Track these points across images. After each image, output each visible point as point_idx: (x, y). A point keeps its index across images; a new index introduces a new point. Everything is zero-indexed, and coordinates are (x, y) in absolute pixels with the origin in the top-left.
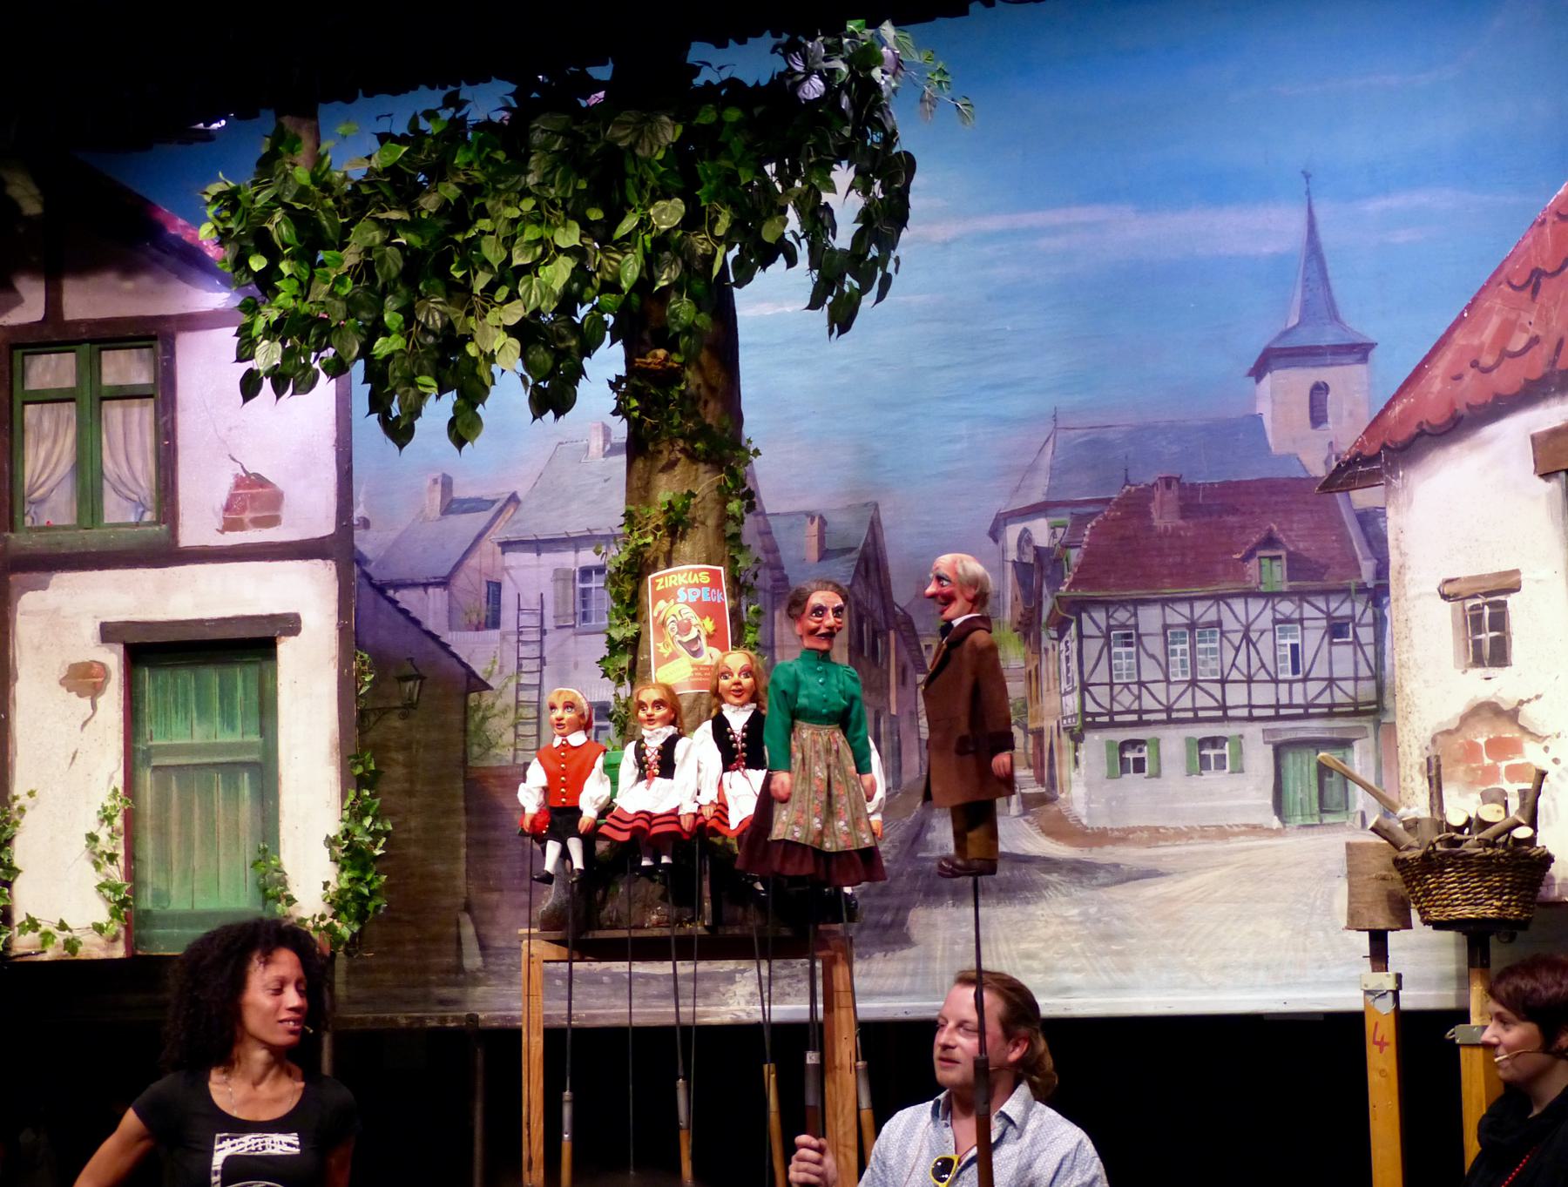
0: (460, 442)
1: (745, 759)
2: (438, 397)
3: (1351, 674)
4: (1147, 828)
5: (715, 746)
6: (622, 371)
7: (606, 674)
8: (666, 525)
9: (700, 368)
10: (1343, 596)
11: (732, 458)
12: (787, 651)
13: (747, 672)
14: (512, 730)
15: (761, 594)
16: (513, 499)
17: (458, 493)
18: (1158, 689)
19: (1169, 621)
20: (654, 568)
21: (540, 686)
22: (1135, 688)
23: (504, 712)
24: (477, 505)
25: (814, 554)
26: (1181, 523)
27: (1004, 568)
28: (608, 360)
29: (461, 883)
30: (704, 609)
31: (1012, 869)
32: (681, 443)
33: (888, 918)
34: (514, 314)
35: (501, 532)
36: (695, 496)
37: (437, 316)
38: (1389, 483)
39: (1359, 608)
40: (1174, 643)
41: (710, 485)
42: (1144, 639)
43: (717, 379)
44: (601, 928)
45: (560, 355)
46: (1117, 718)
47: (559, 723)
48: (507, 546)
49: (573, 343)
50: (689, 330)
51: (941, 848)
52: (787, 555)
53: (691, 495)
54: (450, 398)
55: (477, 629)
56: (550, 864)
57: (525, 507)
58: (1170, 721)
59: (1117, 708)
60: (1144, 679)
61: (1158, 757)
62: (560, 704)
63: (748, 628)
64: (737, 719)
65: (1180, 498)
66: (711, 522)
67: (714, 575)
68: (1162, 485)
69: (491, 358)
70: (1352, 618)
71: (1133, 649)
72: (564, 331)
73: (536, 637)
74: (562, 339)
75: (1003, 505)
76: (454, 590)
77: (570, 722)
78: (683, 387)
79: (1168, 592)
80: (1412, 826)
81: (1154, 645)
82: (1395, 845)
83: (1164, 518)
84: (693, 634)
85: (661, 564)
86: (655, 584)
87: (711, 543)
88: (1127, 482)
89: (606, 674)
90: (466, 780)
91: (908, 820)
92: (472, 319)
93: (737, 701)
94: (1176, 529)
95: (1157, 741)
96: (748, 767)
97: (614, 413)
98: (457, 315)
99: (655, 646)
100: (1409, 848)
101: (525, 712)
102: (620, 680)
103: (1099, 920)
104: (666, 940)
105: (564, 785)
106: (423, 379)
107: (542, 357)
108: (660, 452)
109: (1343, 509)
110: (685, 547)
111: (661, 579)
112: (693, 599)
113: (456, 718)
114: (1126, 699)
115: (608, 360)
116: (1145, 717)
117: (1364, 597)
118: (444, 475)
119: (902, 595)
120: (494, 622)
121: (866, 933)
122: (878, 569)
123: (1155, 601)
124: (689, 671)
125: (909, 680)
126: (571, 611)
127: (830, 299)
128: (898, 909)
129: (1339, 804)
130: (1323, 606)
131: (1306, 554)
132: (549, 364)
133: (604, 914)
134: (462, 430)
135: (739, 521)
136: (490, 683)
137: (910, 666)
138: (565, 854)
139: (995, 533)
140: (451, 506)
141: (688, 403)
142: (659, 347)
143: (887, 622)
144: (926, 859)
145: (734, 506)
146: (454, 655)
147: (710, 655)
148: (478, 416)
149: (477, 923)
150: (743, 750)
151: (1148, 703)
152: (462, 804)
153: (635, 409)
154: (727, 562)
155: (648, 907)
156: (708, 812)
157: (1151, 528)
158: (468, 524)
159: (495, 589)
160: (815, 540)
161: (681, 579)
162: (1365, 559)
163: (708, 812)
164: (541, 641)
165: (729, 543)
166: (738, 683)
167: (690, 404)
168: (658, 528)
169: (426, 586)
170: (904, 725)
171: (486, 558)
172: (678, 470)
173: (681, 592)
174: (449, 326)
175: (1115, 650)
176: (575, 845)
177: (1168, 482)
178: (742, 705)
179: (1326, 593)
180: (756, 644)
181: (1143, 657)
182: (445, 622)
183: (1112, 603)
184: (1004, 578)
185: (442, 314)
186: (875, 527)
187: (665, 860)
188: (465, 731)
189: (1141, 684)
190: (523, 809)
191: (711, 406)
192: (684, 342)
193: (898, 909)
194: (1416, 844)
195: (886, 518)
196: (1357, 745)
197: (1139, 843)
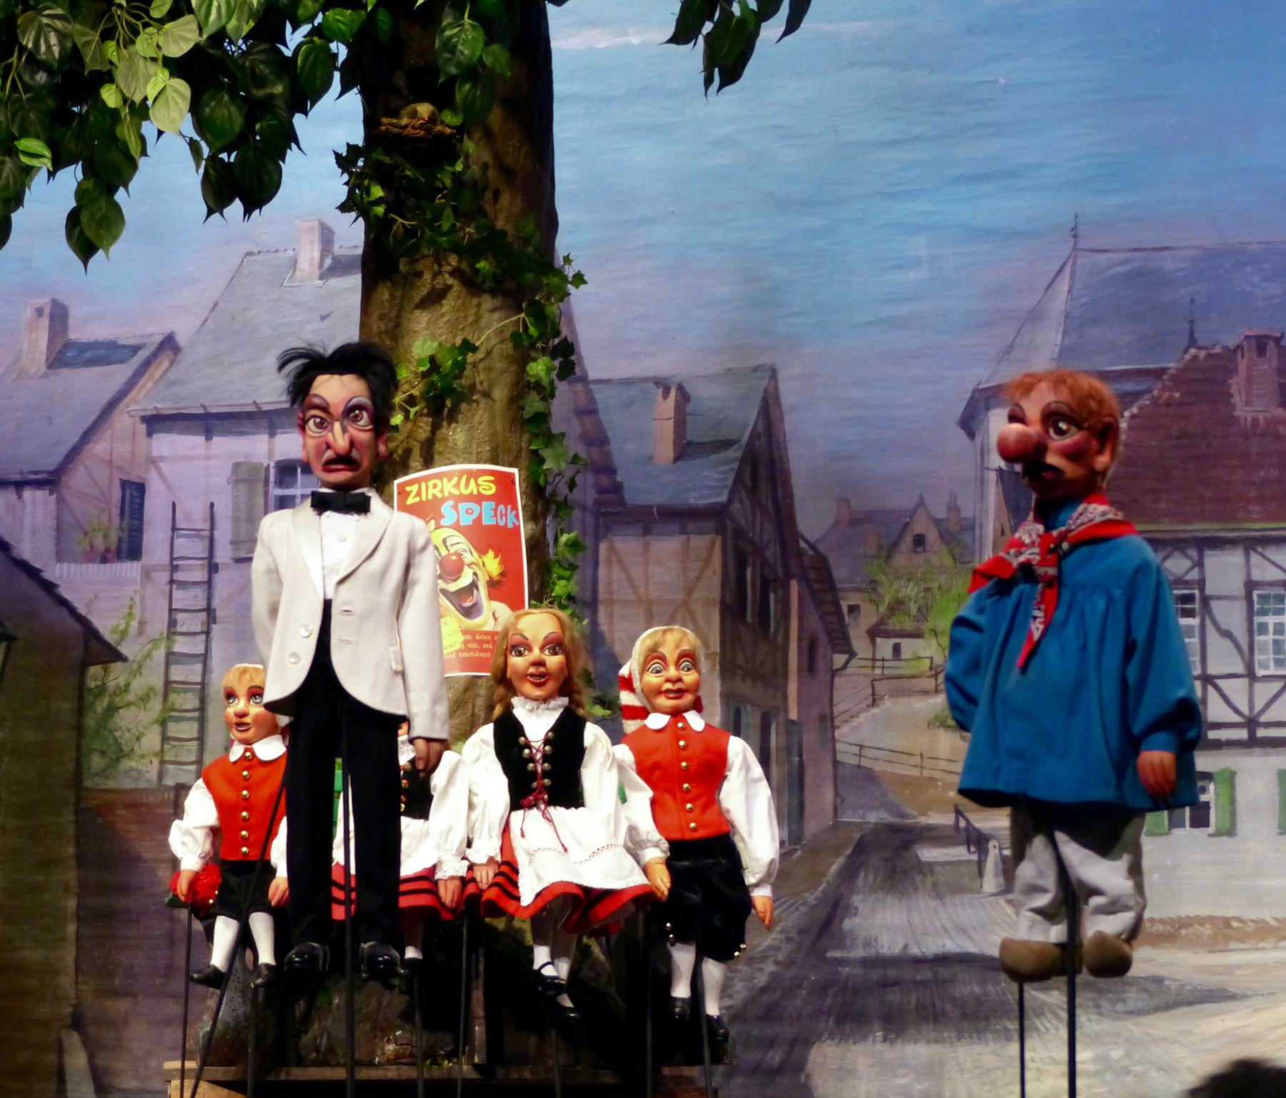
0: (85, 248)
1: (548, 789)
2: (51, 174)
4: (1211, 920)
5: (497, 767)
6: (358, 138)
8: (424, 396)
9: (488, 135)
11: (538, 287)
12: (617, 609)
13: (554, 644)
14: (156, 729)
15: (577, 513)
16: (169, 344)
17: (78, 332)
18: (1237, 689)
19: (1256, 576)
20: (404, 468)
21: (205, 658)
23: (145, 699)
24: (104, 353)
25: (666, 451)
27: (982, 480)
28: (335, 120)
29: (66, 982)
30: (484, 538)
31: (983, 982)
32: (453, 260)
33: (775, 1057)
34: (181, 39)
35: (145, 399)
36: (474, 349)
37: (53, 39)
40: (1264, 613)
41: (501, 331)
42: (1214, 605)
43: (515, 151)
44: (301, 1063)
45: (256, 109)
47: (240, 722)
48: (155, 422)
49: (279, 89)
50: (473, 72)
51: (867, 944)
52: (623, 450)
53: (468, 347)
54: (72, 176)
55: (104, 560)
56: (219, 957)
57: (186, 359)
58: (1253, 742)
60: (1211, 670)
61: (1232, 802)
62: (242, 690)
63: (557, 571)
64: (537, 724)
66: (500, 394)
67: (504, 482)
68: (1251, 353)
69: (141, 111)
71: (1195, 622)
72: (263, 69)
73: (201, 575)
74: (261, 82)
75: (981, 375)
76: (66, 493)
77: (257, 717)
78: (459, 167)
79: (1256, 527)
81: (1231, 615)
83: (1252, 403)
84: (466, 579)
85: (415, 461)
87: (499, 427)
88: (1192, 342)
90: (78, 811)
91: (811, 898)
92: (111, 48)
93: (538, 692)
95: (1230, 777)
96: (553, 802)
97: (344, 208)
98: (87, 37)
101: (178, 700)
103: (1127, 1071)
104: (409, 1085)
105: (246, 824)
106: (26, 144)
107: (227, 112)
108: (419, 275)
110: (456, 434)
112: (467, 521)
113: (65, 707)
115: (335, 120)
118: (55, 303)
119: (813, 520)
120: (131, 548)
121: (739, 1080)
122: (773, 479)
123: (1233, 542)
124: (461, 638)
125: (820, 664)
127: (708, 27)
128: (793, 1043)
132: (238, 123)
133: (306, 1039)
134: (90, 229)
135: (547, 393)
136: (124, 650)
137: (823, 638)
138: (245, 940)
139: (970, 422)
140: (65, 354)
141: (467, 195)
142: (421, 100)
143: (786, 566)
144: (842, 962)
145: (539, 368)
146: (64, 603)
147: (494, 615)
148: (117, 208)
149: (92, 1049)
150: (546, 774)
152: (71, 850)
153: (379, 201)
154: (525, 463)
155: (381, 1030)
156: (485, 877)
158: (93, 385)
159: (134, 495)
160: (669, 428)
161: (448, 487)
163: (485, 877)
164: (209, 583)
165: (527, 431)
166: (540, 663)
167: (472, 200)
168: (411, 401)
169: (19, 485)
170: (810, 738)
171: (121, 441)
172: (448, 304)
173: (447, 509)
174: (74, 55)
176: (261, 925)
177: (1261, 344)
178: (545, 700)
180: (570, 598)
181: (1212, 635)
182: (49, 546)
184: (983, 497)
185: (62, 36)
186: (770, 406)
187: (411, 953)
188: (79, 729)
190: (175, 862)
191: (505, 199)
192: (463, 91)
193: (793, 1043)
195: (789, 393)
197: (1196, 943)
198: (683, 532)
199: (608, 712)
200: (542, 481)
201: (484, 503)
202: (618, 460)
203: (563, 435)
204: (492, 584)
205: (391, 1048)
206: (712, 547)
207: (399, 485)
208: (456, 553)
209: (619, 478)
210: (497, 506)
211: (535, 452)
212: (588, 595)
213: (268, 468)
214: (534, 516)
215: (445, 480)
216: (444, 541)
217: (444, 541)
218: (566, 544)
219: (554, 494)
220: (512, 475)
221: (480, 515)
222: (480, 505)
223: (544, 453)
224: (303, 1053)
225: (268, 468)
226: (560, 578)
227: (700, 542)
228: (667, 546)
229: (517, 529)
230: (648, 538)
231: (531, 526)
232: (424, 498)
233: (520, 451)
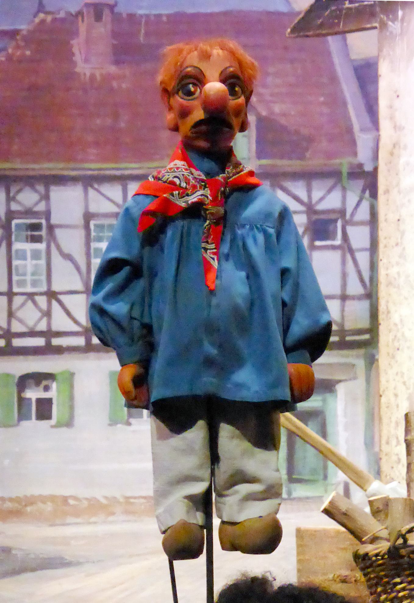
3: (338, 291)
4: (52, 498)
10: (330, 182)
19: (93, 209)
22: (42, 301)
26: (113, 69)
38: (383, 26)
39: (352, 199)
42: (58, 232)
46: (17, 342)
59: (17, 327)
60: (56, 287)
61: (71, 398)
65: (115, 34)
68: (89, 18)
70: (342, 212)
71: (41, 246)
79: (93, 167)
80: (381, 508)
81: (71, 241)
82: (356, 534)
83: (90, 59)
88: (41, 8)
94: (108, 78)
100: (374, 540)
109: (337, 60)
114: (29, 316)
116: (56, 342)
117: (360, 183)
123: (74, 180)
129: (314, 471)
130: (302, 194)
131: (283, 121)
151: (60, 321)
157: (71, 76)
162: (362, 130)
175: (17, 246)
179: (308, 176)
183: (17, 179)
189: (51, 295)
194: (384, 534)
196: (341, 389)
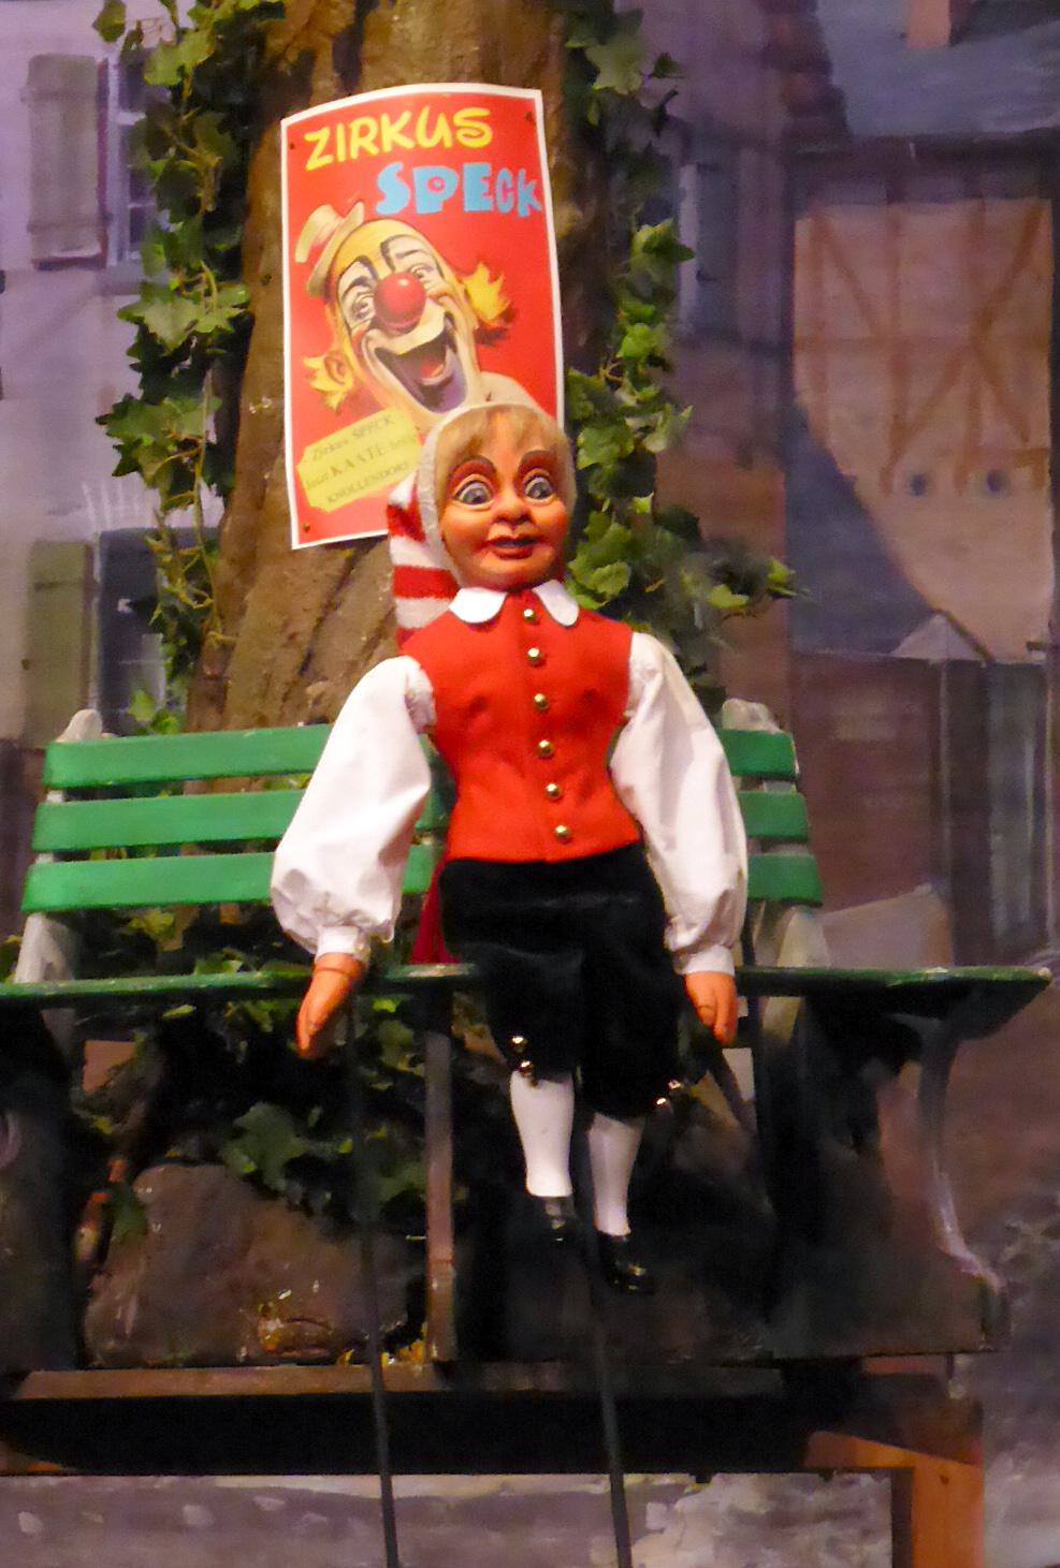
7: (127, 466)
15: (748, 157)
30: (467, 240)
63: (628, 305)
84: (428, 330)
85: (324, 79)
86: (301, 149)
89: (127, 466)
99: (300, 368)
102: (178, 485)
111: (328, 131)
112: (429, 204)
126: (89, 206)
133: (95, 1308)
161: (392, 134)
180: (654, 360)
198: (973, 193)
199: (742, 599)
200: (593, 118)
201: (467, 166)
202: (835, 41)
203: (636, 16)
204: (485, 336)
205: (273, 1326)
206: (1029, 231)
207: (291, 129)
208: (407, 274)
209: (836, 80)
210: (495, 170)
211: (578, 55)
212: (771, 332)
213: (104, 67)
214: (571, 188)
215: (385, 119)
216: (384, 248)
217: (384, 248)
218: (647, 248)
219: (623, 144)
220: (525, 107)
221: (459, 192)
222: (459, 170)
223: (596, 54)
224: (89, 1335)
225: (104, 67)
226: (636, 319)
227: (1004, 214)
228: (936, 225)
229: (537, 218)
230: (895, 209)
231: (569, 211)
232: (341, 157)
233: (544, 55)
